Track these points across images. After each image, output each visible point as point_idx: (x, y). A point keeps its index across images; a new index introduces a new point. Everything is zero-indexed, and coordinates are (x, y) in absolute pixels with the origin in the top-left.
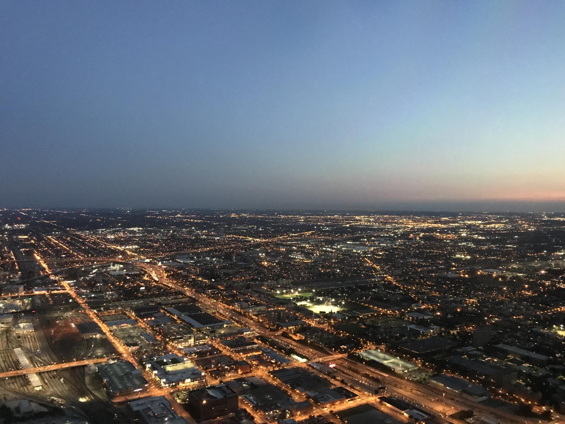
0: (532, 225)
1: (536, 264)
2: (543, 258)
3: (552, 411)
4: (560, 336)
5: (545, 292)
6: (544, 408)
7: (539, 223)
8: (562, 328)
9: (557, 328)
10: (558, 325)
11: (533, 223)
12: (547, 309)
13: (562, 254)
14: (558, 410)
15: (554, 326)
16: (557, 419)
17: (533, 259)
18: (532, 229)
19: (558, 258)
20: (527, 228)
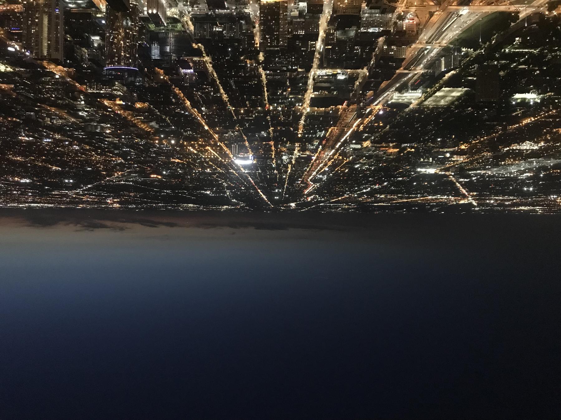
0: (552, 201)
1: (551, 162)
2: (545, 168)
3: (547, 13)
4: (534, 92)
5: (546, 134)
6: (555, 13)
7: (546, 204)
8: (532, 101)
9: (536, 100)
10: (535, 103)
11: (552, 204)
12: (545, 117)
13: (525, 174)
14: (540, 15)
15: (539, 101)
16: (542, 7)
17: (555, 167)
18: (553, 197)
19: (530, 170)
20: (558, 198)
